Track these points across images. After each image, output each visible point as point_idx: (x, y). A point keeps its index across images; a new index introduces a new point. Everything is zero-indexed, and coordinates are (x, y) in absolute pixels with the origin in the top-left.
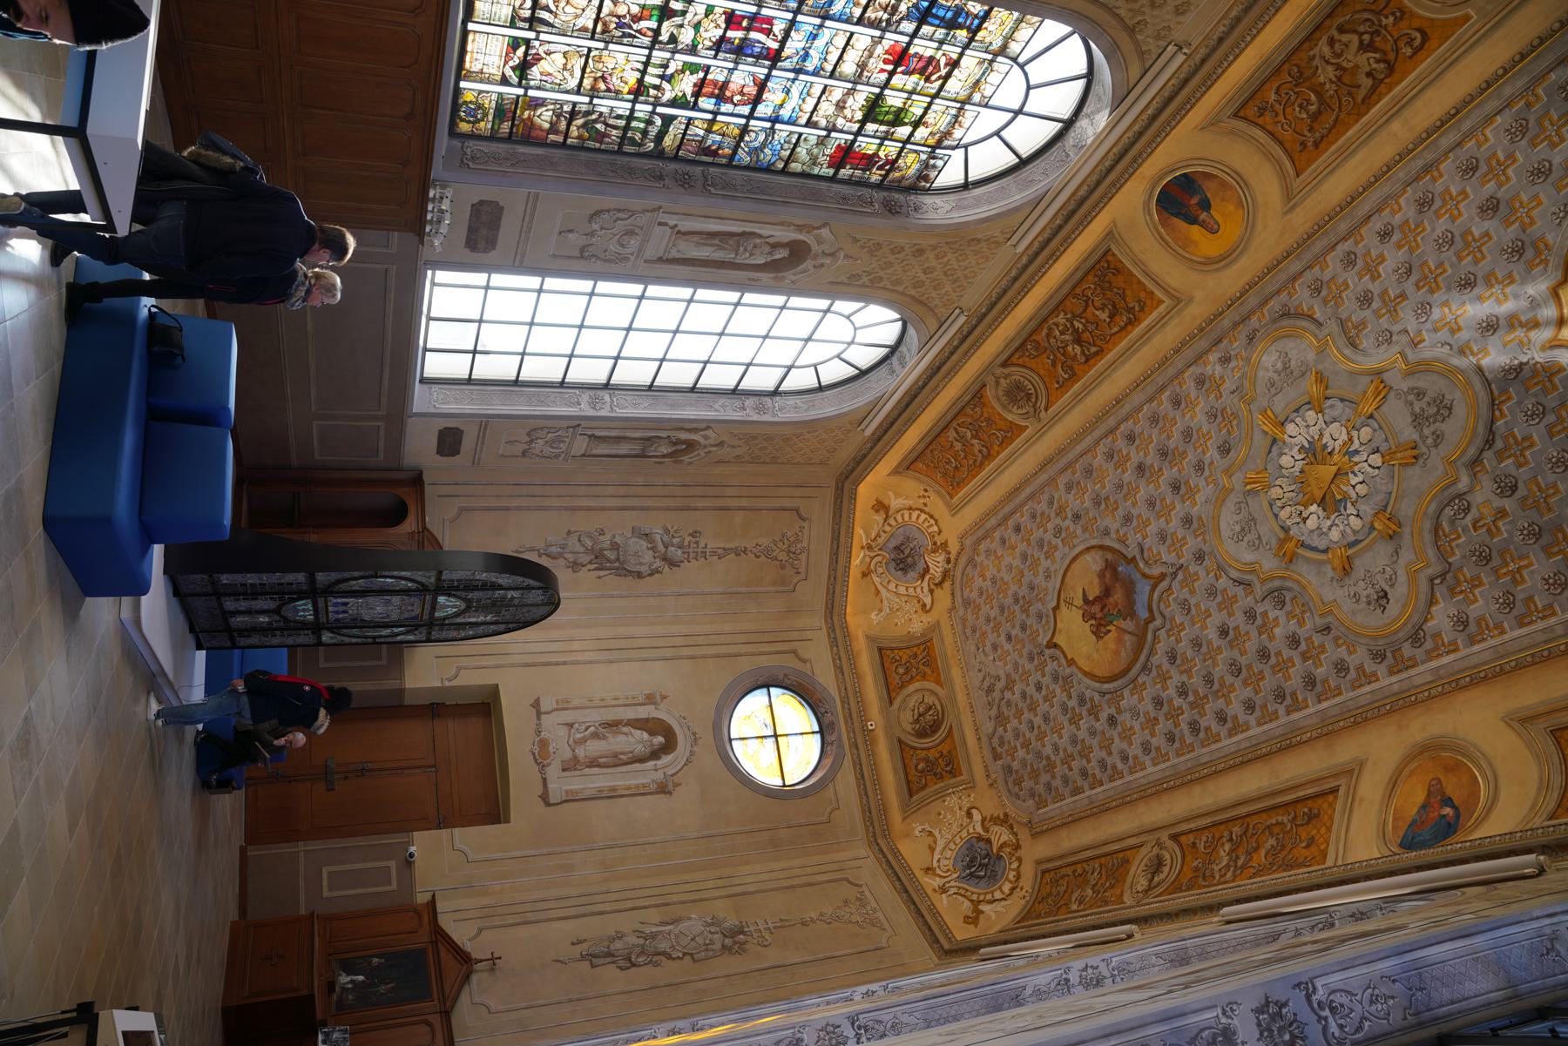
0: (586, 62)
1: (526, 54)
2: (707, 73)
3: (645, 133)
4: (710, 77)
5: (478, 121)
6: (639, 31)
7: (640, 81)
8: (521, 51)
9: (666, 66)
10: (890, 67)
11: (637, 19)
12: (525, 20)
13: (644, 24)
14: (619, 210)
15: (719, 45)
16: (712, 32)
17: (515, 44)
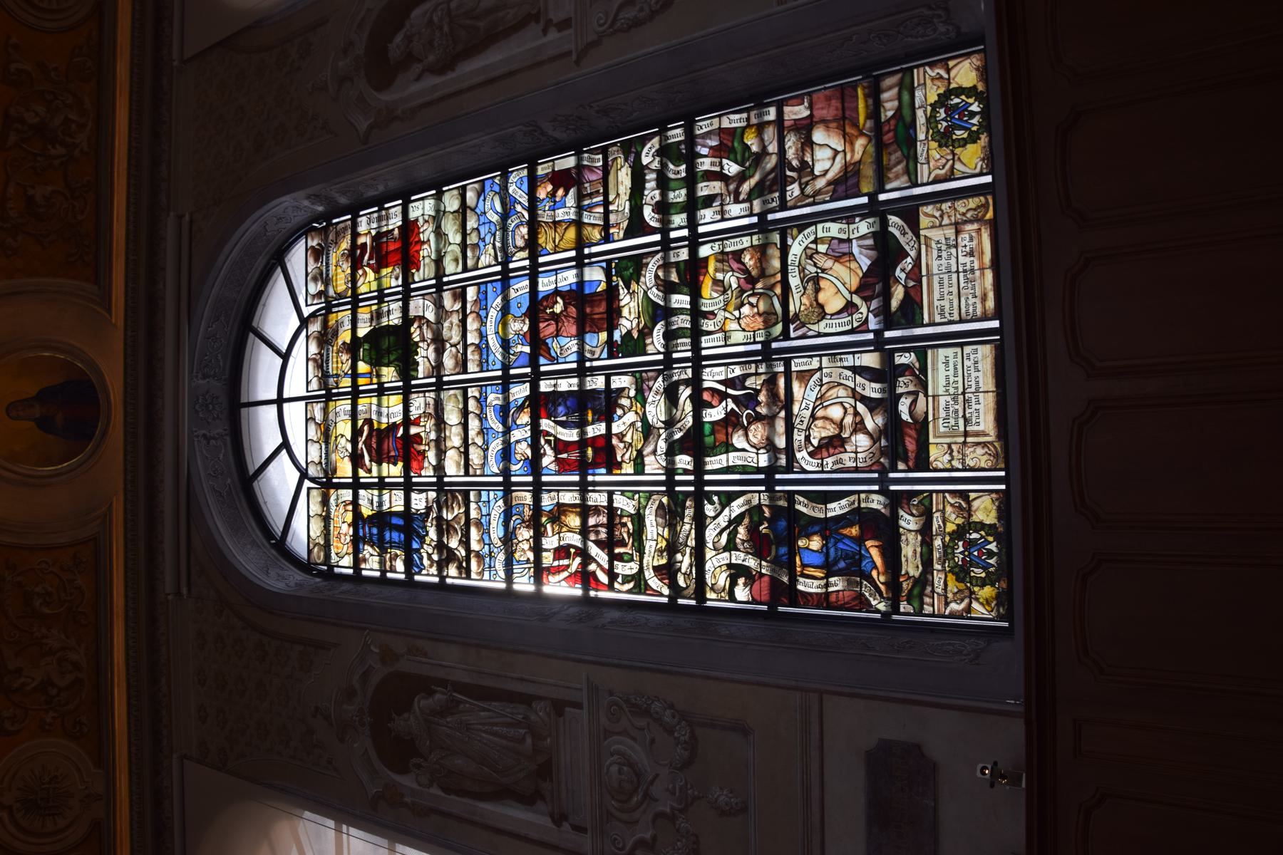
0: (785, 305)
1: (887, 296)
2: (610, 342)
3: (664, 183)
4: (603, 336)
5: (943, 99)
6: (723, 396)
7: (696, 296)
8: (898, 294)
9: (670, 336)
10: (413, 430)
11: (731, 421)
12: (906, 368)
13: (714, 414)
14: (637, 23)
15: (607, 404)
16: (624, 422)
17: (911, 311)
